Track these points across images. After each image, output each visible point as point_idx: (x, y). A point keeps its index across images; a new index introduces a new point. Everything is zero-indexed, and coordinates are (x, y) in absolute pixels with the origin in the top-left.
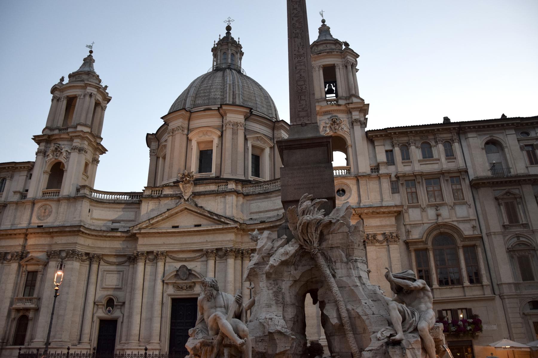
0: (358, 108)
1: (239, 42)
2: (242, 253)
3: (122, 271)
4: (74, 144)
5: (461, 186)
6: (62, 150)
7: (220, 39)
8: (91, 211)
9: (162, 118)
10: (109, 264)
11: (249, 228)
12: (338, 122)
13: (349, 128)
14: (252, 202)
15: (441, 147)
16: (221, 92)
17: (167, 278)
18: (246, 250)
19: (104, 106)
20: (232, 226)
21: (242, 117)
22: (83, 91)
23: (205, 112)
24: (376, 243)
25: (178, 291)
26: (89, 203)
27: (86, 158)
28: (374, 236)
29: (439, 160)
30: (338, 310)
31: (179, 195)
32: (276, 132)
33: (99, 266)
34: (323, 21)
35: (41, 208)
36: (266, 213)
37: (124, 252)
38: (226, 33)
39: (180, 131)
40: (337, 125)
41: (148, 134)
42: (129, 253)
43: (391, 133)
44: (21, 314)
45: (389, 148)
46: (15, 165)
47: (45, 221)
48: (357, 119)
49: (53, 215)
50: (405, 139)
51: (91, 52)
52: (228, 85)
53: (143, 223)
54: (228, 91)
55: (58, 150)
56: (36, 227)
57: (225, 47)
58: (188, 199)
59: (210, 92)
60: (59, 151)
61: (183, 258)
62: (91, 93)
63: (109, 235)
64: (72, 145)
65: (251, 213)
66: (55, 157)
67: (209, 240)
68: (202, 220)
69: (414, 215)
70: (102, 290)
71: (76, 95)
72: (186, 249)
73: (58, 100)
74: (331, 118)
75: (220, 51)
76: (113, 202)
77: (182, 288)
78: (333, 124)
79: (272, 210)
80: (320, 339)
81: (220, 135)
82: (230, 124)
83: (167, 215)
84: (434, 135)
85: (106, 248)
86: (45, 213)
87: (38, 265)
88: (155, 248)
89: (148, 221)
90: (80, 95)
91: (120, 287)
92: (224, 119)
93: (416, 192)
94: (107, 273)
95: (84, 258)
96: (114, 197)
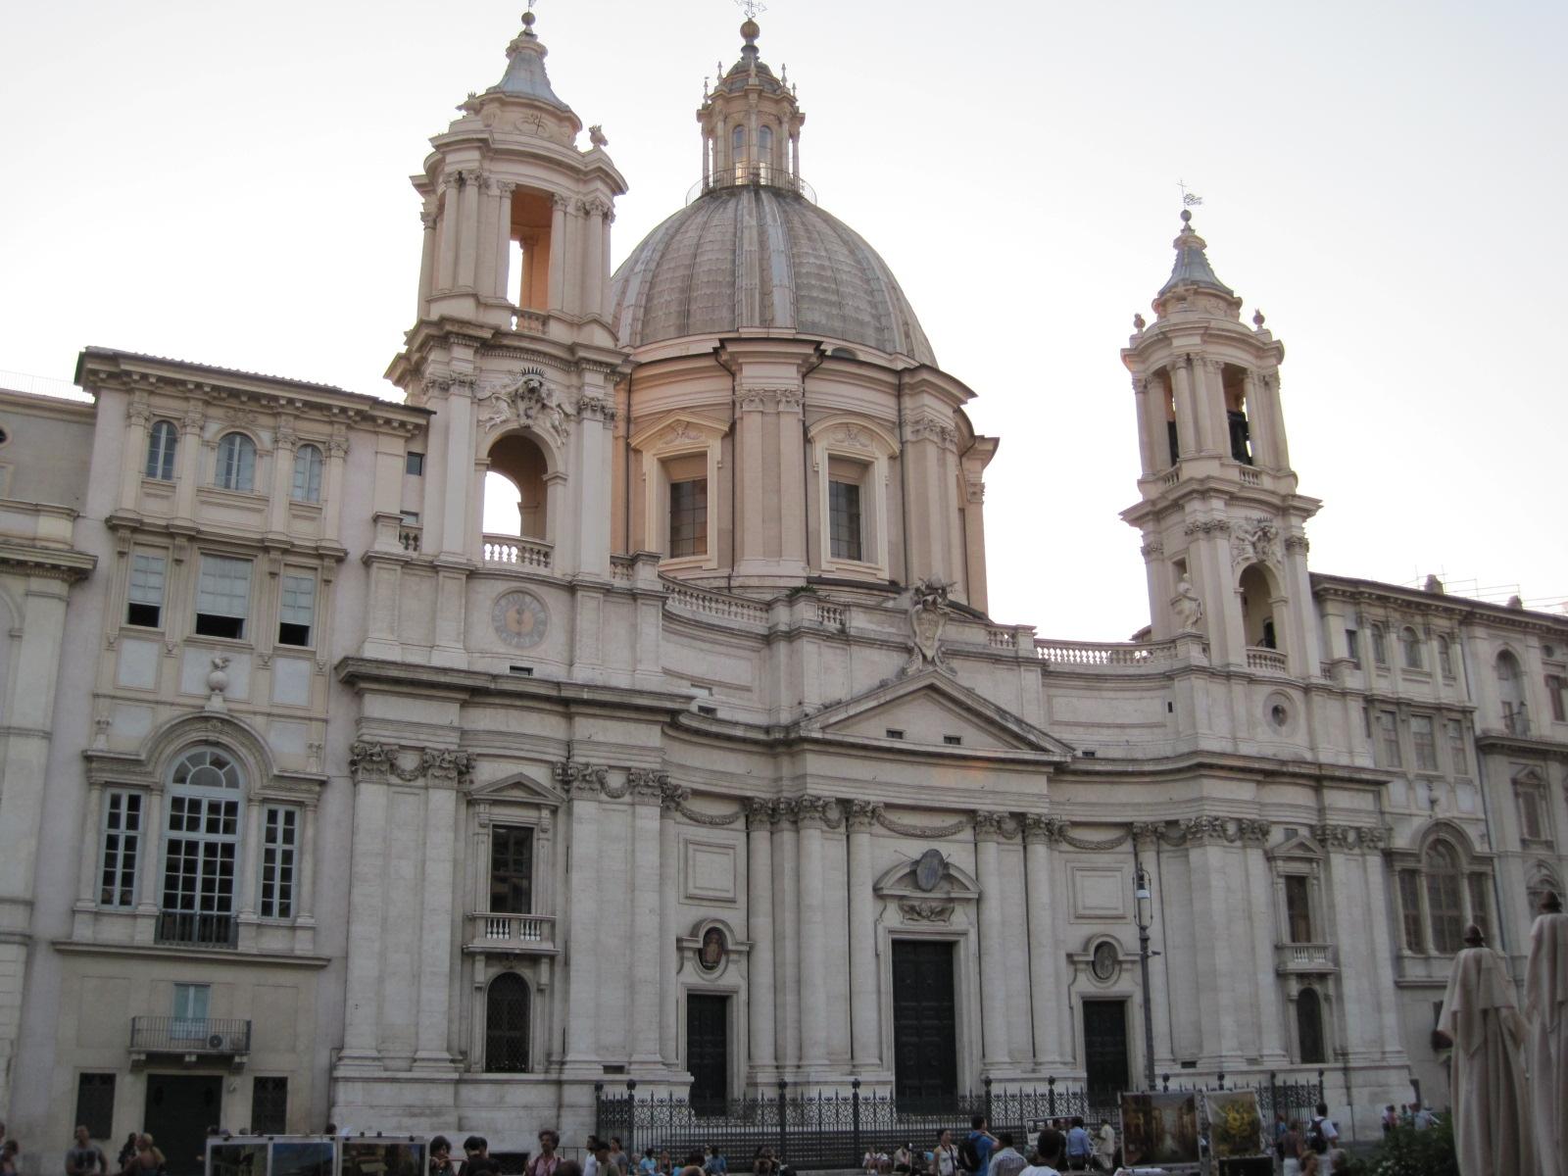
4: (590, 392)
5: (1463, 743)
14: (1053, 691)
15: (1435, 644)
16: (870, 302)
20: (1056, 759)
28: (1345, 830)
29: (1429, 675)
31: (899, 639)
32: (964, 460)
34: (1186, 216)
35: (503, 602)
36: (1091, 730)
37: (741, 789)
42: (763, 795)
43: (1361, 593)
44: (495, 971)
45: (1352, 627)
50: (1378, 612)
51: (528, 19)
55: (532, 394)
56: (508, 672)
60: (537, 401)
61: (915, 827)
64: (580, 388)
66: (524, 421)
68: (963, 725)
69: (1396, 791)
70: (686, 901)
71: (552, 195)
74: (1259, 521)
77: (919, 914)
79: (1108, 726)
80: (1261, 1056)
81: (898, 452)
83: (888, 698)
84: (1425, 615)
86: (519, 622)
87: (538, 806)
91: (730, 895)
92: (908, 402)
93: (1397, 742)
94: (695, 850)
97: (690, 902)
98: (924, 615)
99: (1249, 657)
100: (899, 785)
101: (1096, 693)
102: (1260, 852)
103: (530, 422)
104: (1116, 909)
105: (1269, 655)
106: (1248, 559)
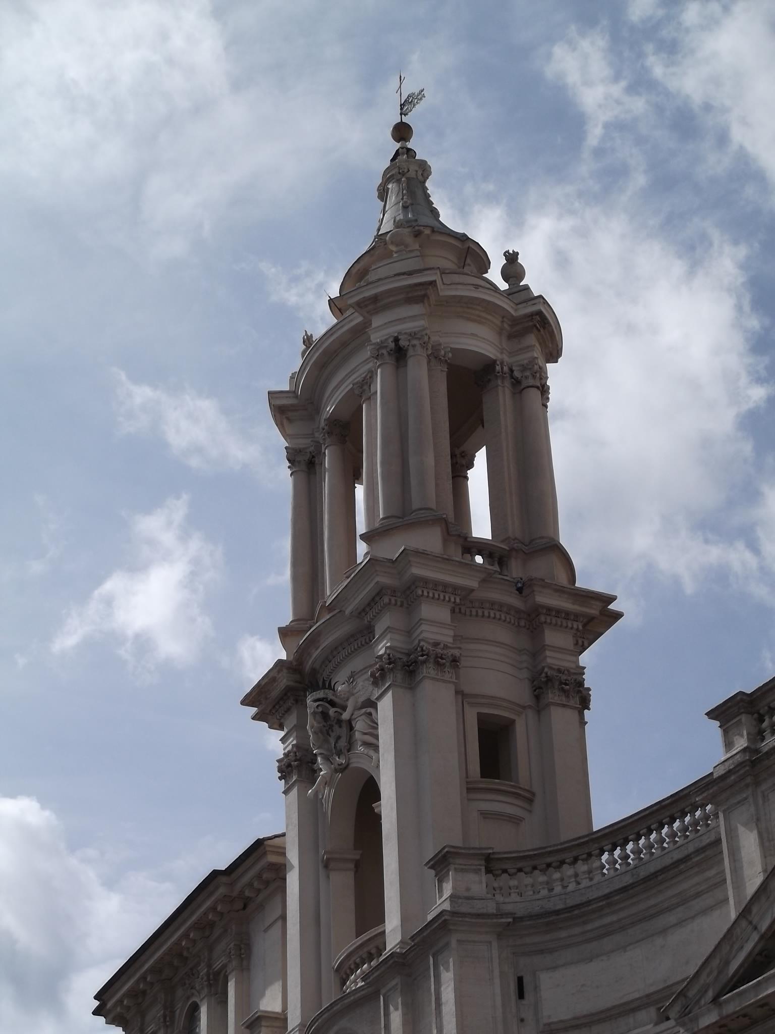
6: (344, 708)
8: (527, 987)
19: (524, 368)
22: (367, 352)
26: (495, 944)
27: (459, 692)
51: (402, 132)
76: (628, 880)
89: (744, 923)
96: (637, 852)
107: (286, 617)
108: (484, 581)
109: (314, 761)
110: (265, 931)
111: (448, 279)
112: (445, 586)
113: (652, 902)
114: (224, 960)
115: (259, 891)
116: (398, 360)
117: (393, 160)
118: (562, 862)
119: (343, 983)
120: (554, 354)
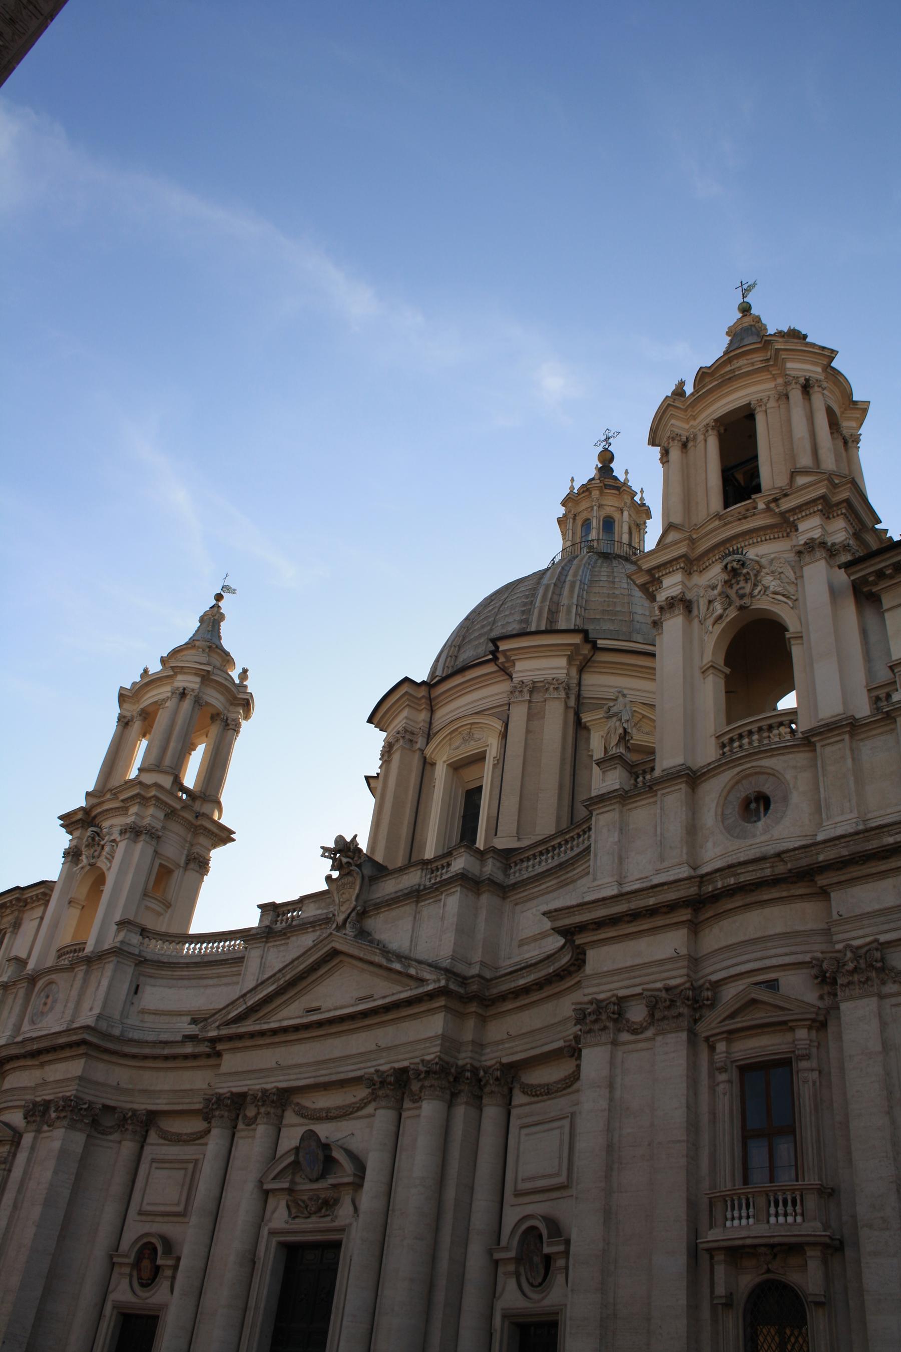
0: (814, 501)
1: (626, 480)
2: (480, 1080)
3: (187, 1161)
4: (130, 820)
6: (103, 839)
7: (572, 488)
8: (140, 990)
9: (370, 720)
10: (170, 1140)
11: (495, 991)
12: (745, 571)
13: (793, 580)
17: (272, 1176)
18: (490, 1067)
19: (233, 720)
20: (430, 987)
21: (563, 662)
23: (465, 676)
24: (883, 983)
25: (297, 1220)
26: (133, 967)
30: (712, 1292)
33: (142, 1147)
38: (600, 470)
39: (401, 742)
40: (746, 580)
41: (368, 778)
46: (23, 894)
47: (40, 1026)
48: (812, 540)
49: (59, 1007)
51: (219, 597)
52: (541, 591)
53: (230, 1007)
54: (538, 604)
55: (96, 840)
57: (584, 505)
58: (345, 921)
59: (494, 622)
61: (321, 1109)
62: (184, 689)
63: (166, 1051)
65: (522, 943)
67: (383, 1046)
70: (139, 1218)
72: (326, 1079)
73: (127, 724)
75: (574, 519)
76: (198, 960)
78: (733, 581)
82: (521, 692)
83: (288, 977)
85: (161, 1091)
86: (45, 1004)
88: (256, 1081)
90: (165, 700)
94: (157, 1168)
95: (108, 1121)
96: (206, 948)
97: (143, 1218)
98: (340, 883)
99: (723, 746)
100: (299, 1066)
101: (571, 887)
102: (684, 1035)
103: (94, 861)
104: (558, 1174)
105: (764, 724)
106: (720, 617)
107: (91, 789)
108: (183, 807)
109: (80, 855)
110: (31, 920)
111: (216, 671)
112: (166, 804)
113: (205, 972)
114: (7, 925)
115: (33, 902)
116: (182, 697)
117: (211, 608)
118: (173, 941)
119: (59, 957)
120: (247, 717)
